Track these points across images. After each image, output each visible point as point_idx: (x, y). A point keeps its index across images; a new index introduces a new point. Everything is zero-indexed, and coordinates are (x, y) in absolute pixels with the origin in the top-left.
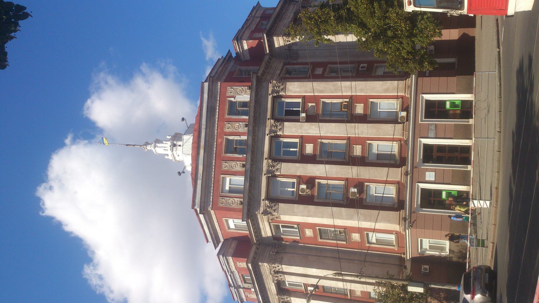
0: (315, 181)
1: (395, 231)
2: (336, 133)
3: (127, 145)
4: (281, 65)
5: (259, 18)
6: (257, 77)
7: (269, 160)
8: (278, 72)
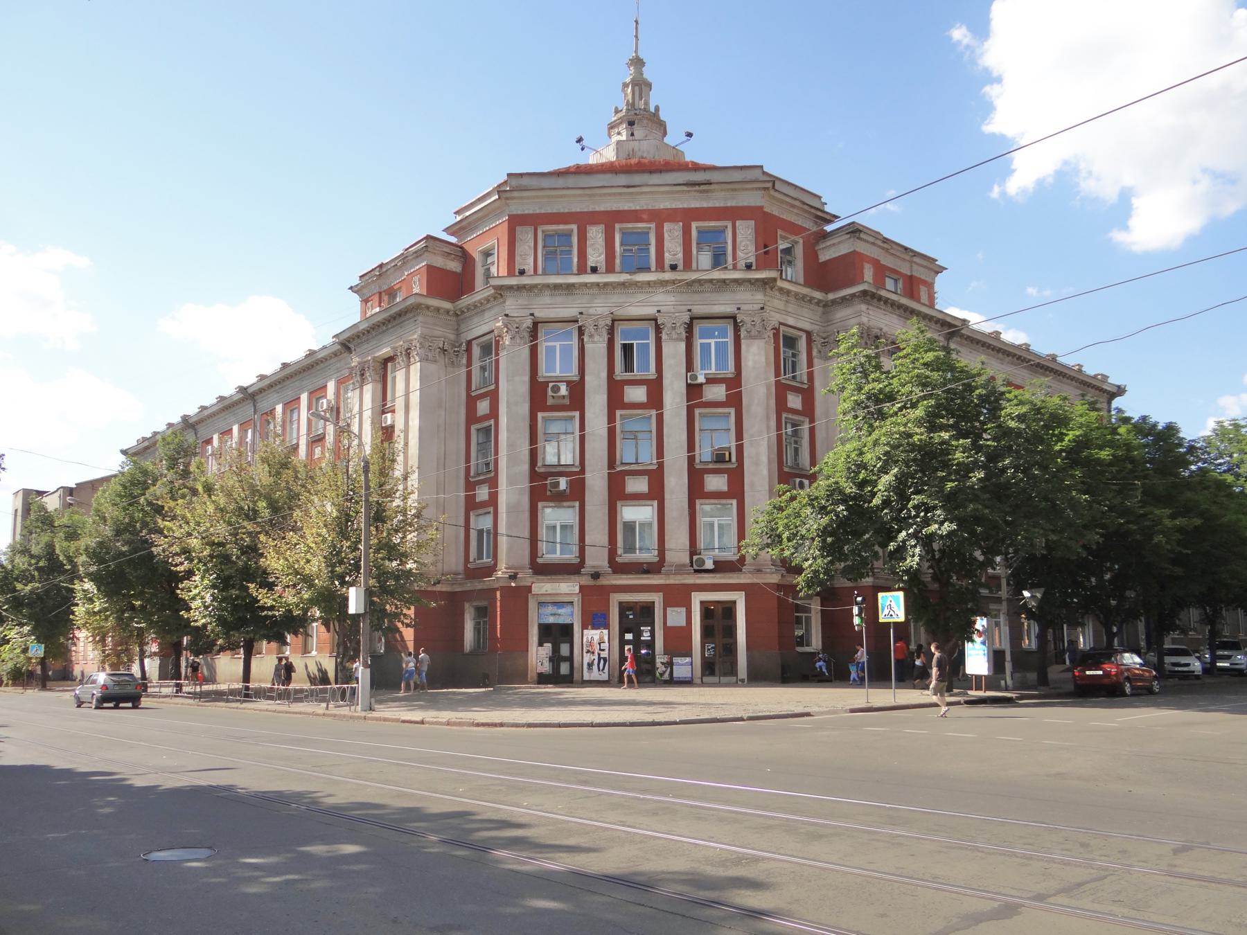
1: (496, 565)
3: (637, 22)
4: (807, 326)
5: (909, 274)
6: (775, 280)
8: (791, 321)
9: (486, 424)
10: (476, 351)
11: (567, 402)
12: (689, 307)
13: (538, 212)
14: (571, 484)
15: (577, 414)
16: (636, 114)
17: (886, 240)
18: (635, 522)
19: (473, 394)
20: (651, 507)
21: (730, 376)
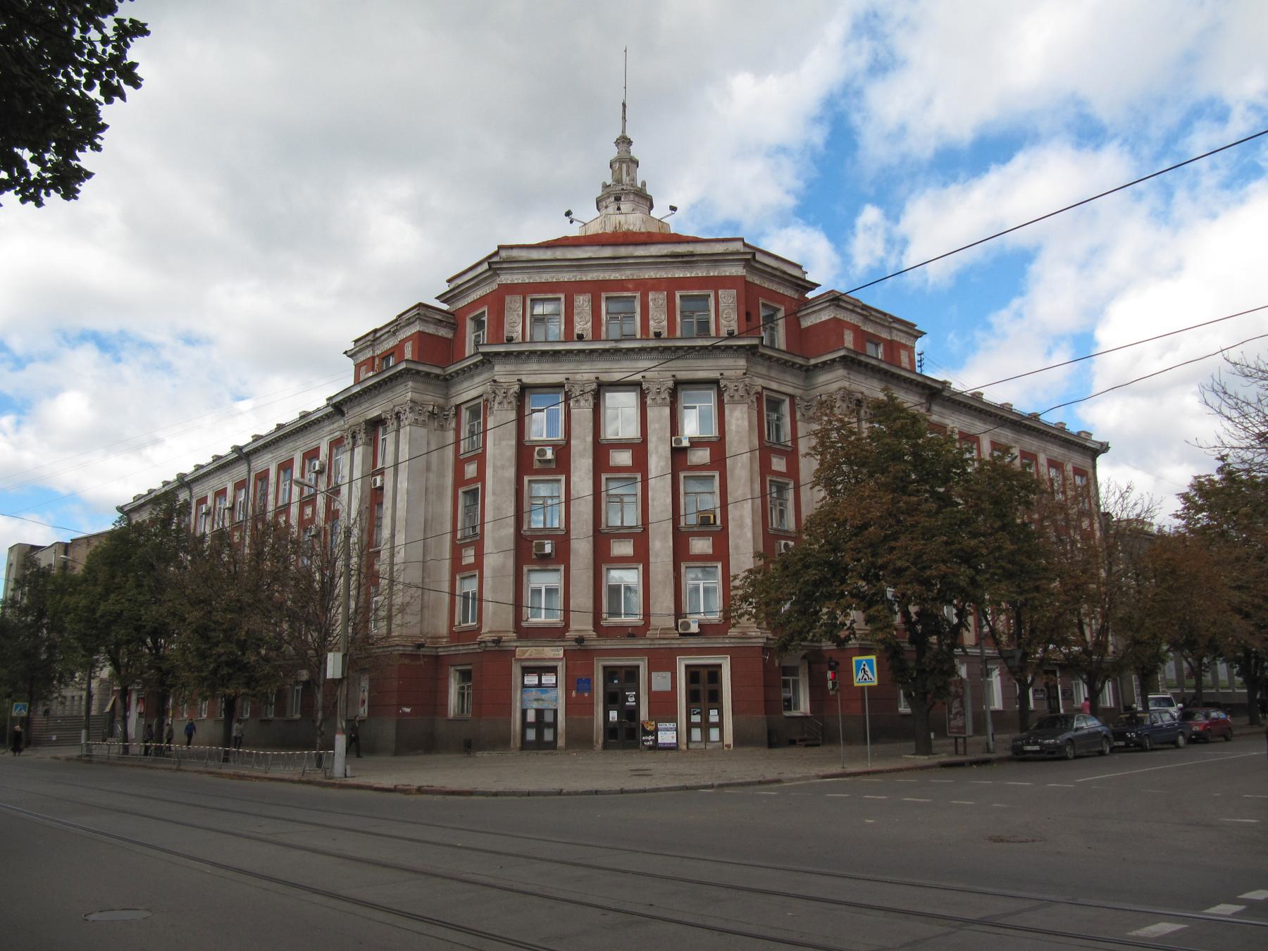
0: (561, 473)
1: (480, 628)
2: (653, 506)
3: (624, 105)
4: (790, 390)
5: (889, 338)
6: (754, 347)
7: (595, 384)
8: (774, 386)
9: (473, 487)
10: (465, 415)
11: (553, 466)
12: (674, 373)
13: (527, 281)
14: (556, 548)
15: (563, 478)
16: (623, 189)
17: (865, 307)
18: (620, 586)
19: (462, 457)
20: (636, 571)
21: (714, 439)
